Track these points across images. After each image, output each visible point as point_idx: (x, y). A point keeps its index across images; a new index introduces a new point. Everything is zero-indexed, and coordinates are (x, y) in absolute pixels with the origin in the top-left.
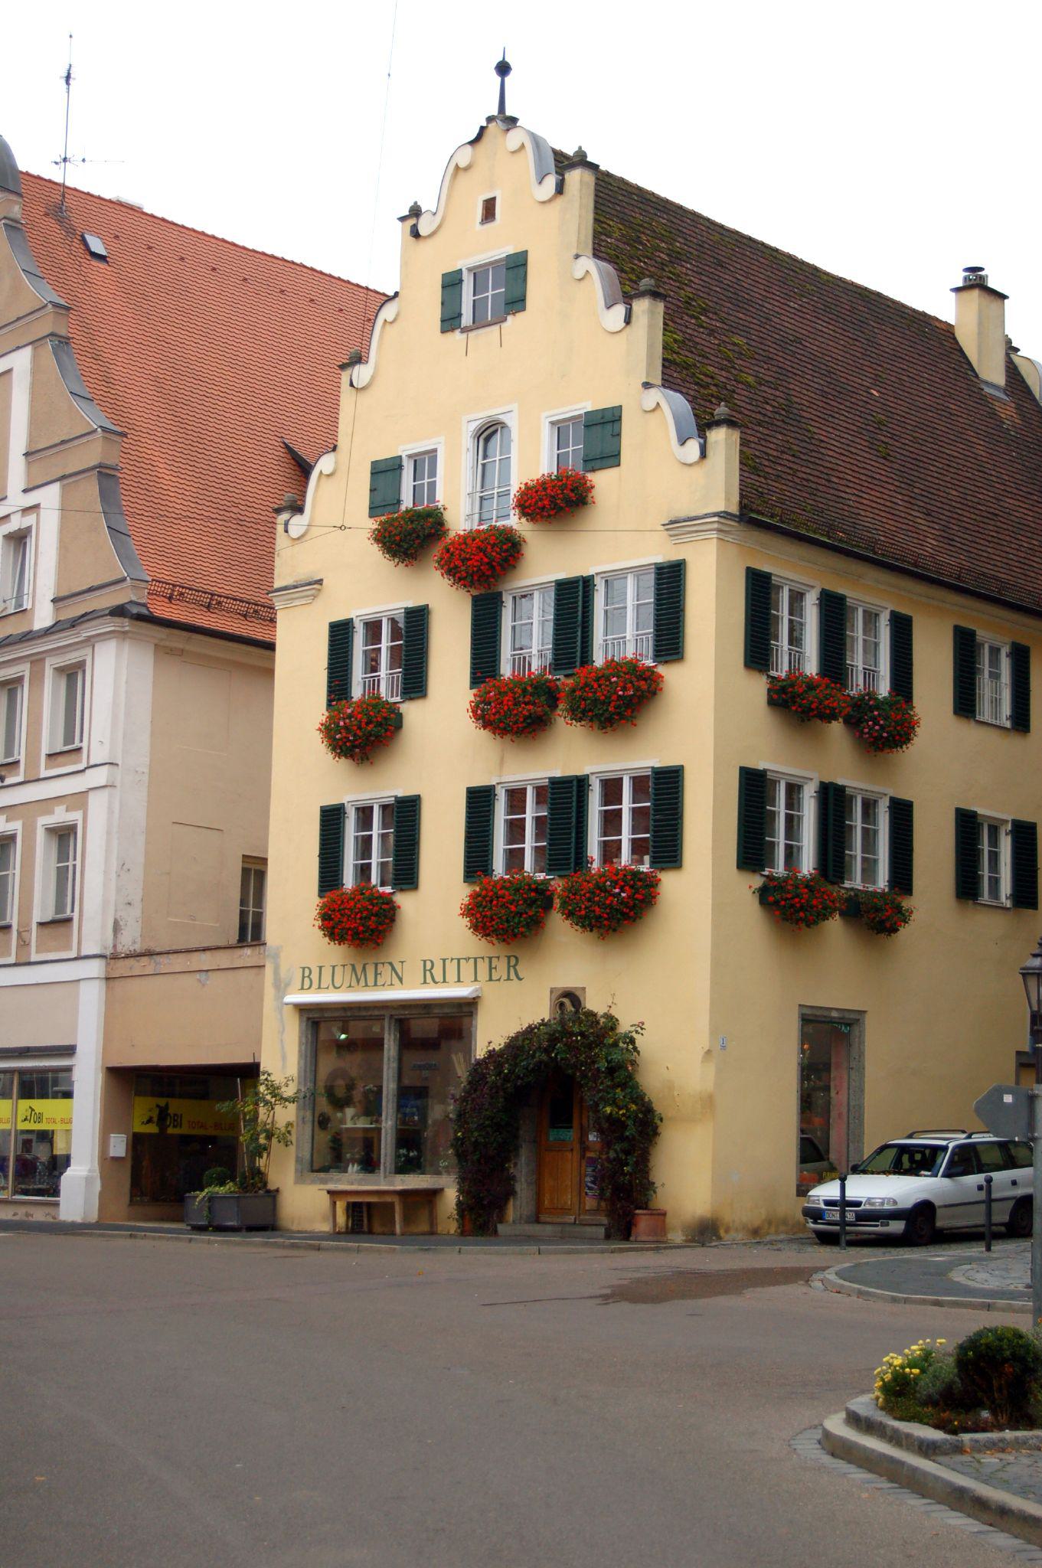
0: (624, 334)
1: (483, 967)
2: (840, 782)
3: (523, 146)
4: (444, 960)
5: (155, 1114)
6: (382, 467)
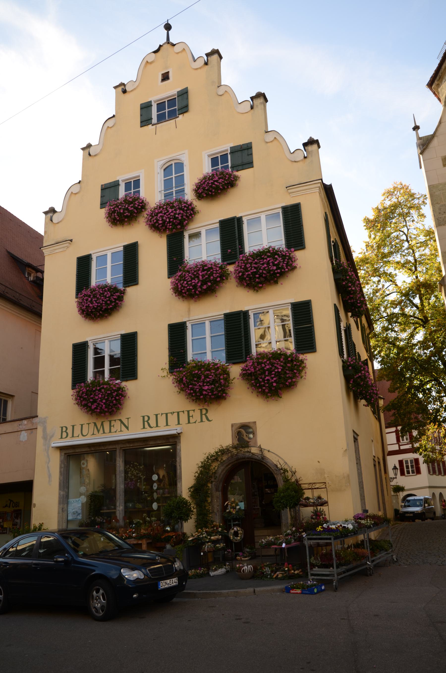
1: (184, 418)
4: (157, 415)
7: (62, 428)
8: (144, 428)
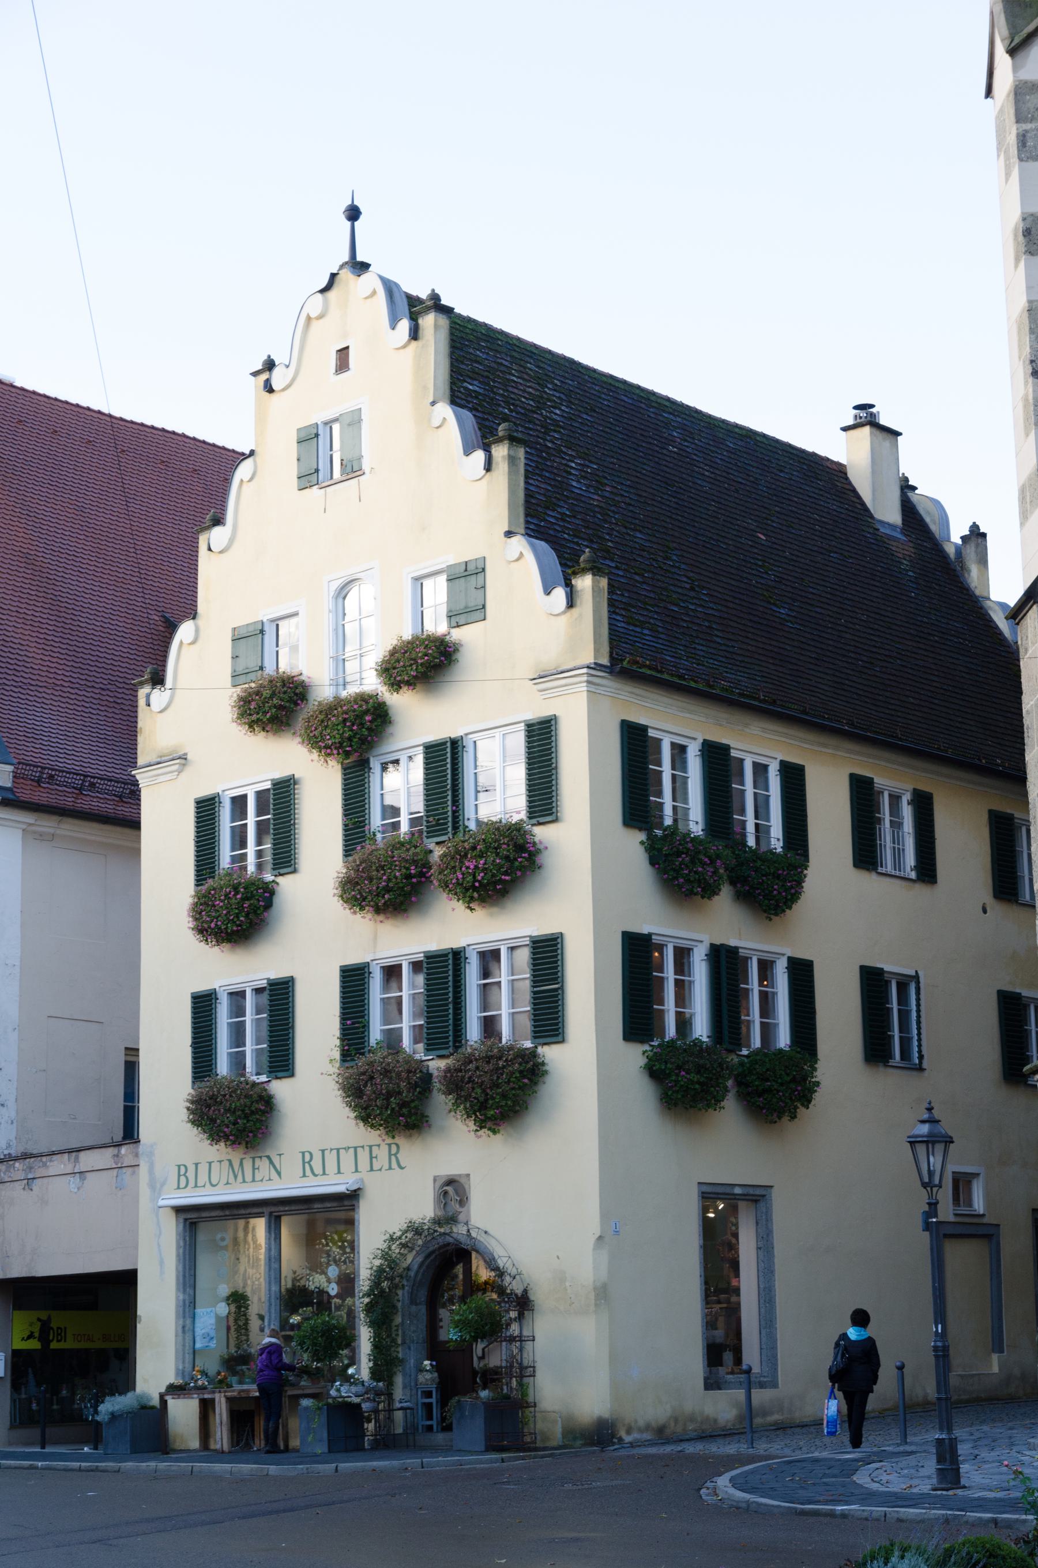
0: (484, 481)
1: (364, 1156)
2: (733, 942)
3: (374, 293)
4: (323, 1151)
5: (36, 1330)
6: (243, 632)
7: (179, 1166)
8: (304, 1175)
